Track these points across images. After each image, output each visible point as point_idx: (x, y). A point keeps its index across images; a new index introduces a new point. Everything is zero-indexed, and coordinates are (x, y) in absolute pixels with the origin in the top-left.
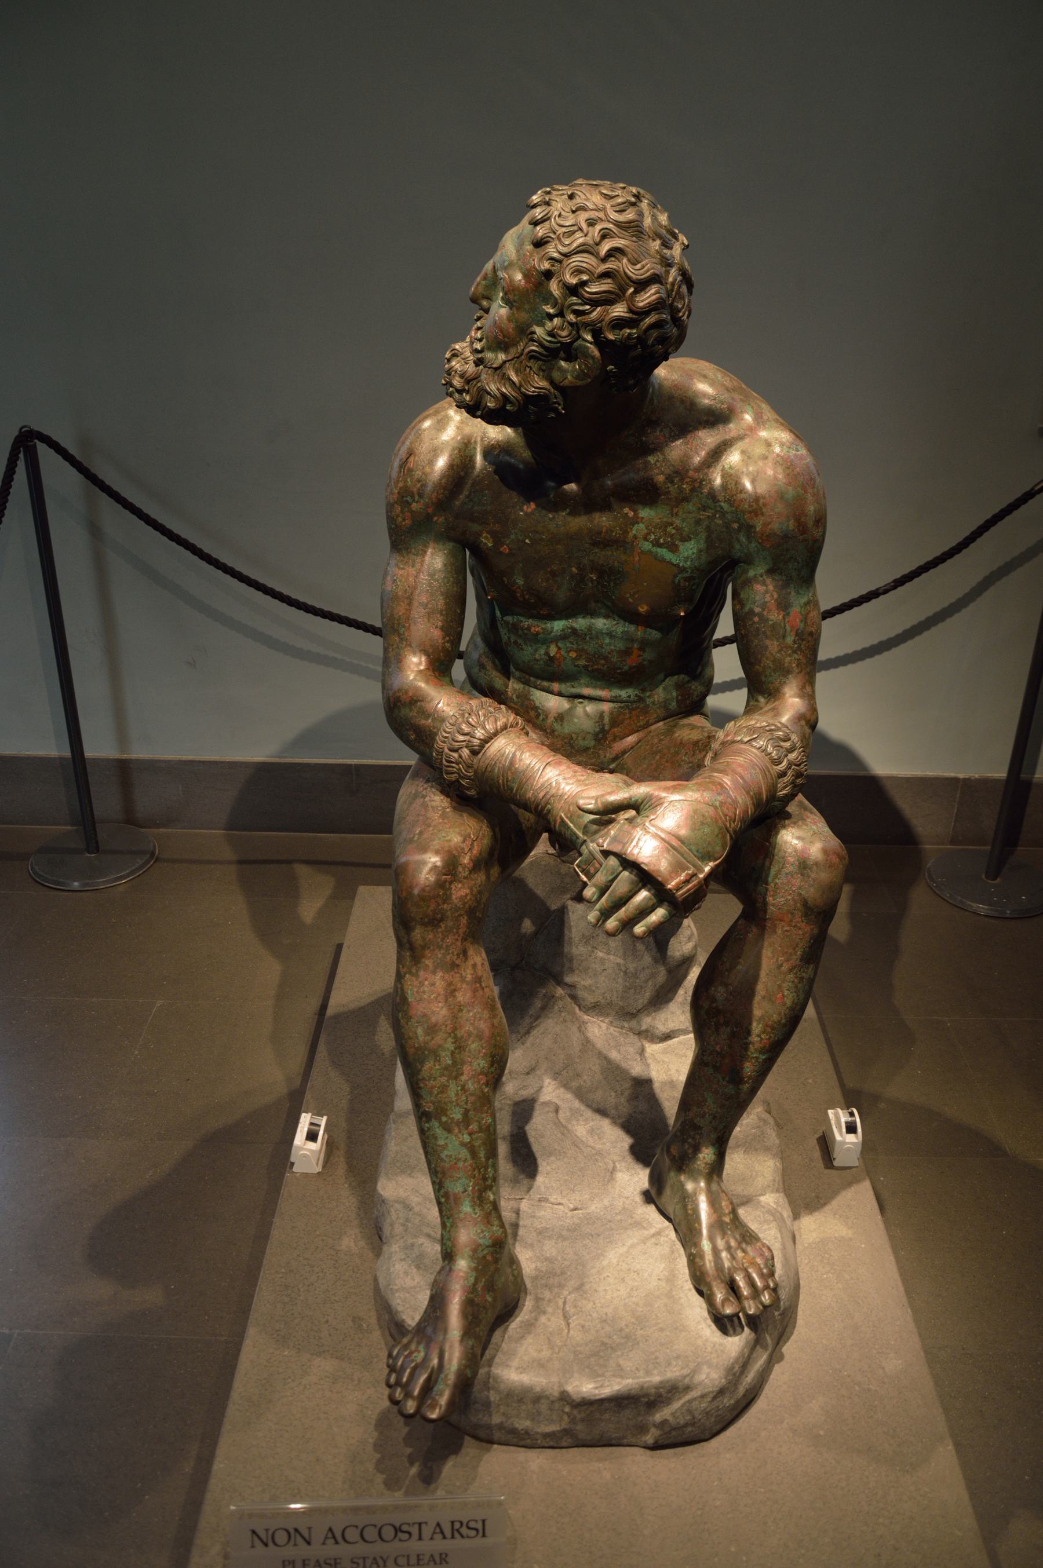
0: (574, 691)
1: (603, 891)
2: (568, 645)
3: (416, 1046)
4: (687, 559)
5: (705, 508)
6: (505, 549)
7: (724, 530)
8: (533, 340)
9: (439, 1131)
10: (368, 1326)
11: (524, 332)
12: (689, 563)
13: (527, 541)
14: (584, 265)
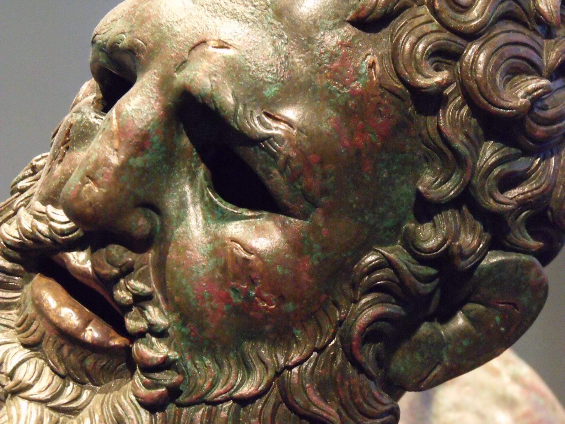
14: (522, 51)
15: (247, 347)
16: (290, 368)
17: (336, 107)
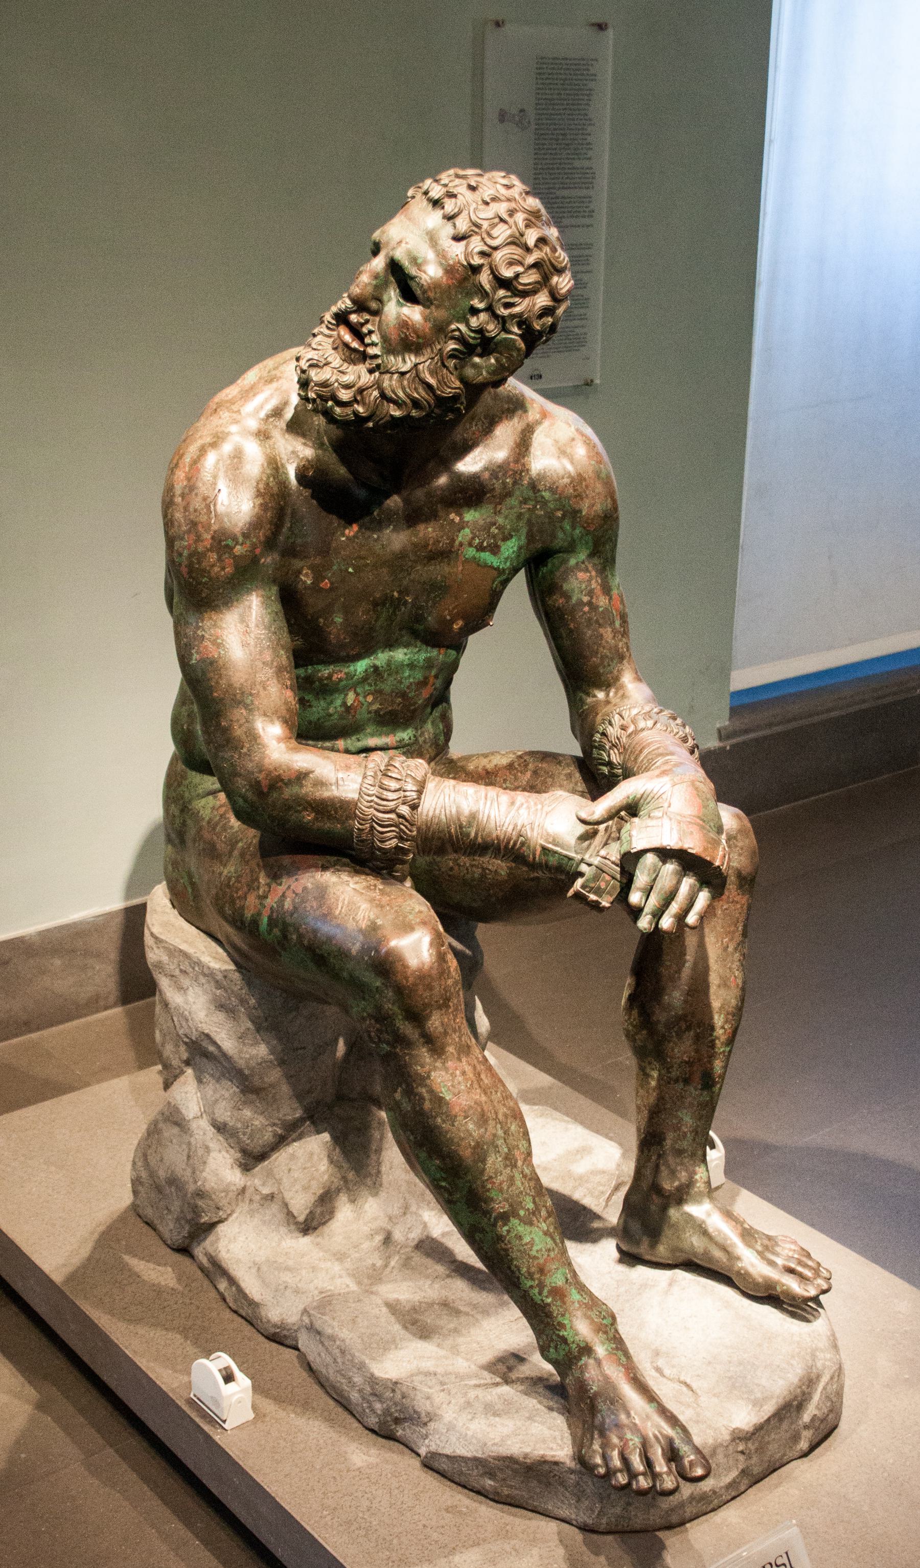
0: (360, 745)
1: (648, 892)
2: (367, 688)
3: (473, 1144)
4: (506, 559)
5: (525, 501)
6: (326, 584)
7: (547, 520)
9: (521, 1229)
10: (467, 1507)
12: (508, 564)
13: (350, 570)
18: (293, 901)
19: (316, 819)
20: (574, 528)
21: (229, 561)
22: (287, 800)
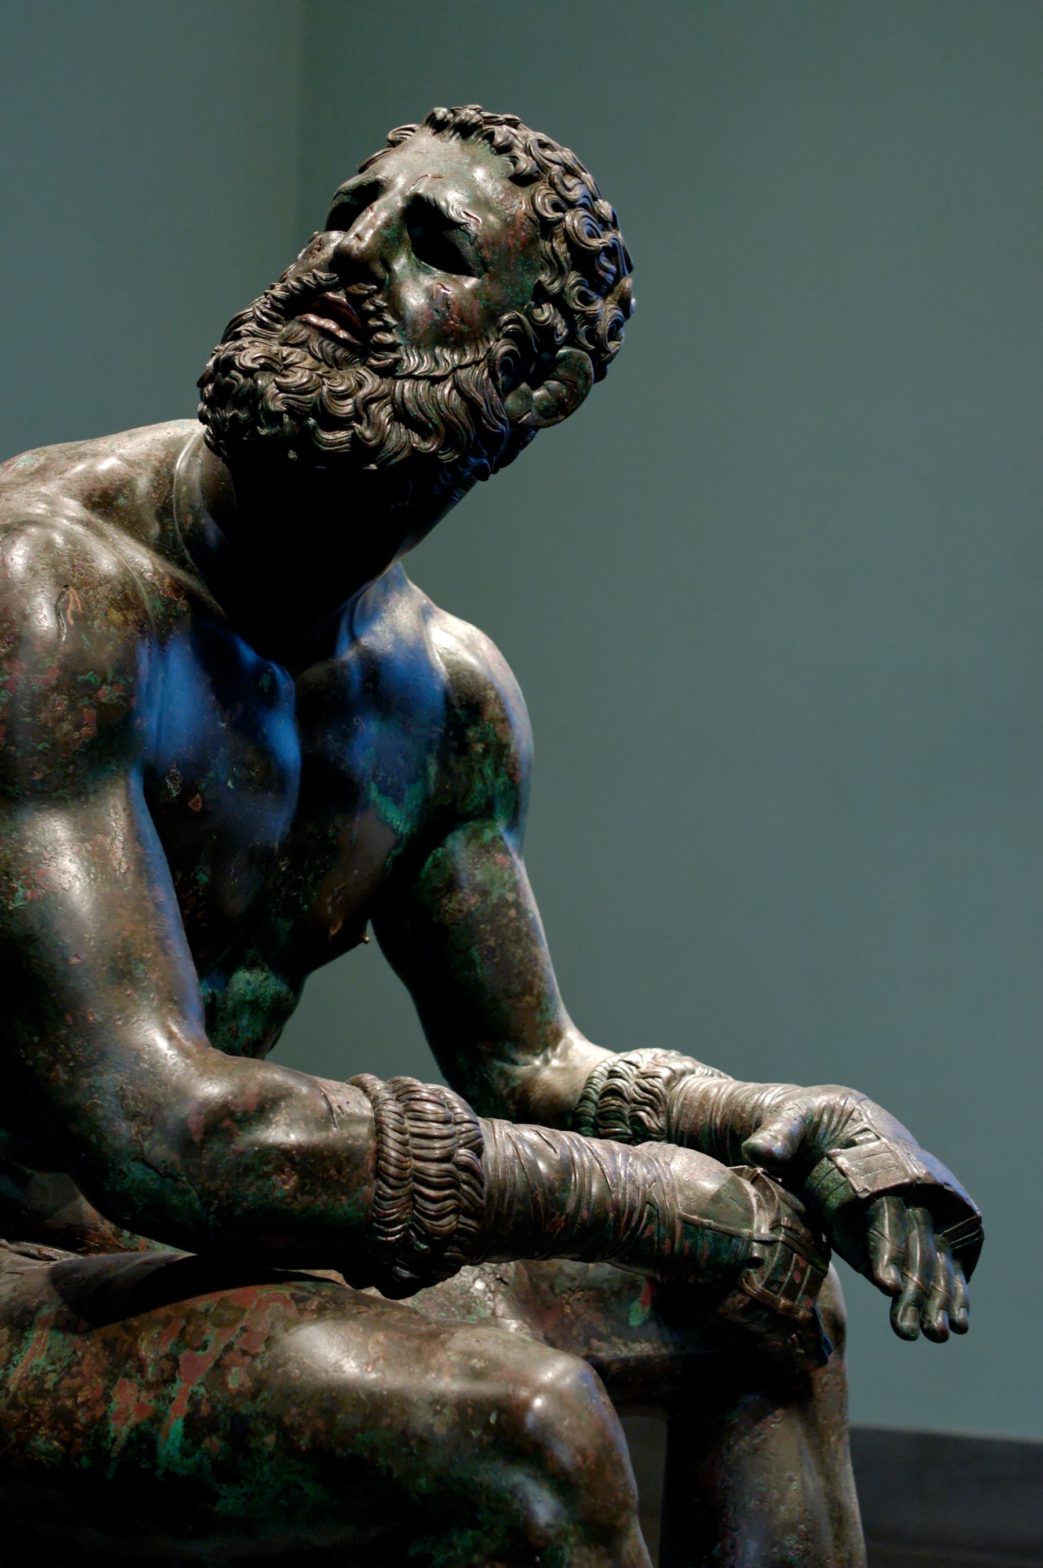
8: (507, 335)
11: (491, 316)
13: (230, 784)
15: (437, 351)
16: (461, 367)
17: (501, 220)
18: (250, 1370)
19: (300, 1188)
20: (497, 775)
21: (89, 713)
22: (242, 1154)
